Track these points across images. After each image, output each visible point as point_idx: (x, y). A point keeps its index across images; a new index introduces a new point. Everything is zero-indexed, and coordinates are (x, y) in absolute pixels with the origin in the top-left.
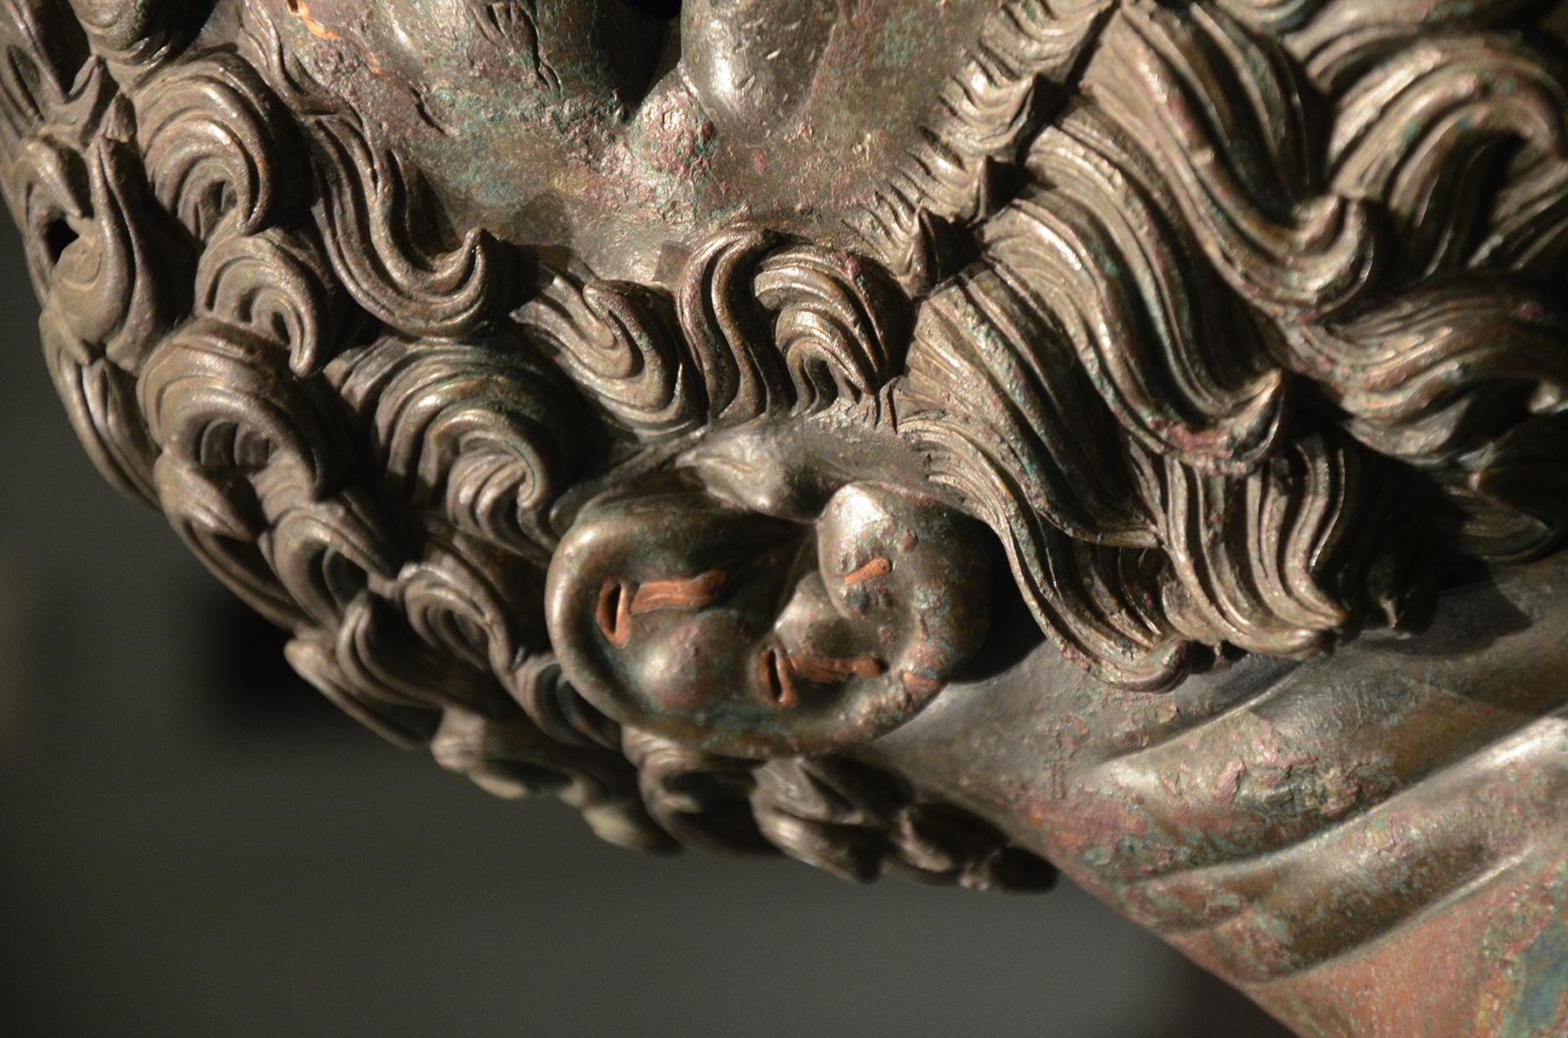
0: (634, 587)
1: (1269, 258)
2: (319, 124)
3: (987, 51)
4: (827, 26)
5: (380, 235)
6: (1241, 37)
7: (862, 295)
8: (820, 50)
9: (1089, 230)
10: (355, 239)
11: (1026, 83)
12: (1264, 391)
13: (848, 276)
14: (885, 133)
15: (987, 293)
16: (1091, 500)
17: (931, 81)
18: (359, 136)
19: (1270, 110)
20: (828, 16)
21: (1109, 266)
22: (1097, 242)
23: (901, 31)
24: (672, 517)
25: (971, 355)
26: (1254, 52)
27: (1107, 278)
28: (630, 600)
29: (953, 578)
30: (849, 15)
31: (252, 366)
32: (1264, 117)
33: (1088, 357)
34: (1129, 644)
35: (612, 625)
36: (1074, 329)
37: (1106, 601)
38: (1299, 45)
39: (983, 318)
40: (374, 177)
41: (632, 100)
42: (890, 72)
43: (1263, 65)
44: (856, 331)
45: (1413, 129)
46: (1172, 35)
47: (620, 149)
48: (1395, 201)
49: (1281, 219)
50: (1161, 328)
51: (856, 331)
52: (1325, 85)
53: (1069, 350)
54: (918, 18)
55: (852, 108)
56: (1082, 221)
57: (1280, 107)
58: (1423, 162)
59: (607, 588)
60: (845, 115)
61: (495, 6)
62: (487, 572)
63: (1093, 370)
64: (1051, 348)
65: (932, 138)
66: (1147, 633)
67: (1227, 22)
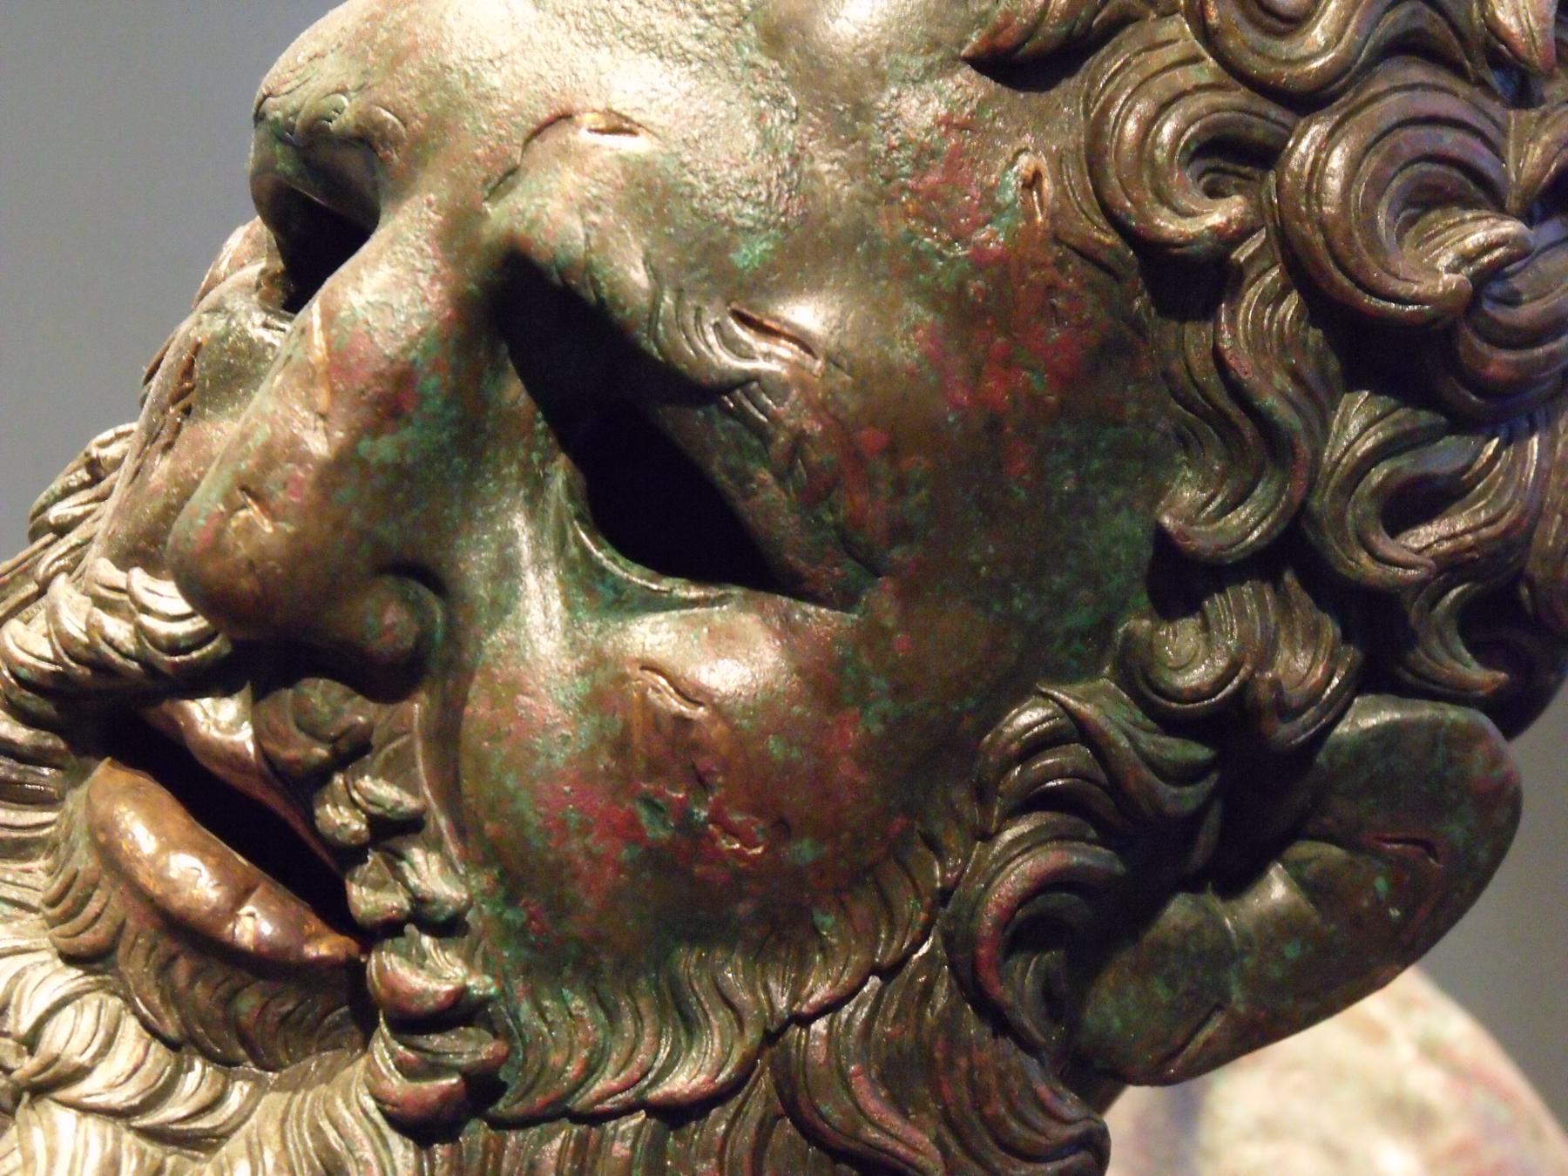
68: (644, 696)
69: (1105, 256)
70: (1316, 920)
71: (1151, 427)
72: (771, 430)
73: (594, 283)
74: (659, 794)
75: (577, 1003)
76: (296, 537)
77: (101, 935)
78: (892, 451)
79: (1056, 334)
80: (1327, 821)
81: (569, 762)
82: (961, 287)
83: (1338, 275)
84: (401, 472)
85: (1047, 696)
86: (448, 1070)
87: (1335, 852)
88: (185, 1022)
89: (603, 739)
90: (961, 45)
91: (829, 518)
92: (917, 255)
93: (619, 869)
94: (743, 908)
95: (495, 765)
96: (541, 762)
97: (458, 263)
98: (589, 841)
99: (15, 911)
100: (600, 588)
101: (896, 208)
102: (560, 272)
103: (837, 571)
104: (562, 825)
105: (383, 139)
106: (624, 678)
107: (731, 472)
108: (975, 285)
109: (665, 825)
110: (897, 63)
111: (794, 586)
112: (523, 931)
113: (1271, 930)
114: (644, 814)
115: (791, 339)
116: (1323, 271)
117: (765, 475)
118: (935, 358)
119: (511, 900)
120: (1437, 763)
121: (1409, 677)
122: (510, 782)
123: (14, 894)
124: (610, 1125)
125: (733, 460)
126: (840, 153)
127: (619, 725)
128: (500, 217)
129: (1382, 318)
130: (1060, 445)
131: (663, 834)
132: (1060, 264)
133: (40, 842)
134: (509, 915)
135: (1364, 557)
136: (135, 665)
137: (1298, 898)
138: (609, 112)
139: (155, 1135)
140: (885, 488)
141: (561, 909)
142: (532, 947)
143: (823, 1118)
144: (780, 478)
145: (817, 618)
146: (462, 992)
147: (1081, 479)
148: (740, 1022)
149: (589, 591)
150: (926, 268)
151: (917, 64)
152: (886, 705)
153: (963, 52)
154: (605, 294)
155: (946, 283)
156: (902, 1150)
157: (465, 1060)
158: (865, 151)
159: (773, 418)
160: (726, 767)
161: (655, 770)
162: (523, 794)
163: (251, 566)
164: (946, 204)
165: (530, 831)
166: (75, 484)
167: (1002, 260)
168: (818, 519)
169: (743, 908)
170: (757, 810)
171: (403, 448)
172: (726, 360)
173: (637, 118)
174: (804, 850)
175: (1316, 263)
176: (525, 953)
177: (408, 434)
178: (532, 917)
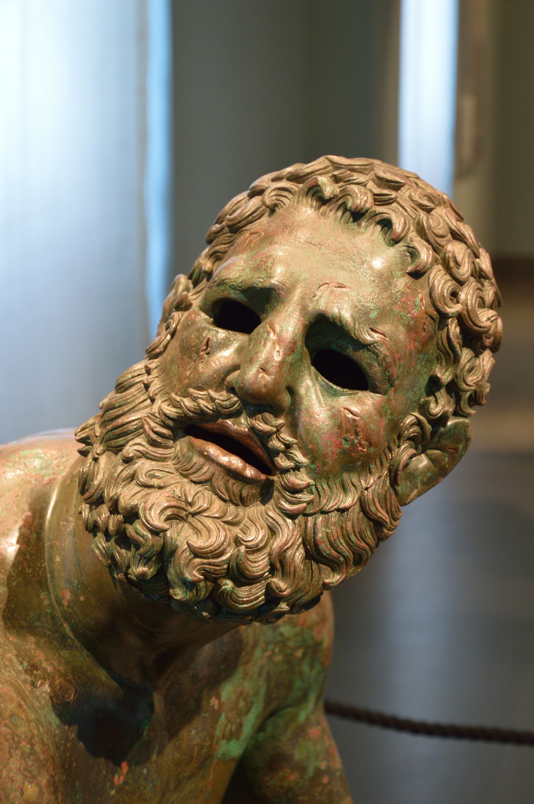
6: (128, 439)
9: (126, 402)
10: (220, 242)
13: (158, 350)
19: (116, 442)
21: (117, 405)
22: (122, 403)
26: (124, 441)
32: (114, 441)
39: (133, 377)
43: (121, 443)
44: (151, 349)
56: (129, 401)
65: (163, 372)
68: (345, 415)
69: (434, 317)
70: (433, 467)
71: (433, 355)
72: (380, 354)
73: (340, 321)
74: (348, 437)
75: (325, 487)
76: (275, 379)
77: (208, 476)
78: (400, 359)
79: (424, 334)
80: (439, 445)
81: (328, 430)
82: (409, 323)
83: (470, 322)
84: (292, 364)
85: (413, 415)
86: (303, 502)
87: (438, 452)
88: (229, 496)
89: (335, 425)
90: (406, 269)
91: (387, 374)
92: (401, 316)
93: (337, 455)
94: (359, 463)
95: (312, 432)
96: (322, 431)
97: (303, 317)
98: (332, 448)
99: (169, 474)
100: (331, 391)
101: (397, 305)
102: (333, 318)
103: (385, 386)
104: (327, 445)
105: (278, 289)
106: (340, 411)
107: (368, 364)
108: (412, 323)
109: (348, 444)
110: (395, 274)
111: (375, 390)
112: (315, 470)
113: (426, 470)
114: (344, 442)
115: (381, 334)
116: (467, 321)
117: (376, 364)
118: (405, 338)
119: (313, 463)
120: (462, 431)
121: (461, 412)
122: (316, 435)
124: (330, 514)
125: (369, 361)
126: (386, 293)
127: (340, 422)
129: (477, 332)
130: (419, 359)
131: (348, 446)
132: (426, 318)
133: (170, 458)
134: (312, 466)
135: (464, 385)
136: (211, 412)
137: (430, 462)
138: (338, 283)
139: (226, 522)
140: (397, 367)
141: (324, 464)
142: (317, 474)
143: (371, 511)
144: (379, 365)
145: (377, 397)
146: (309, 483)
147: (421, 366)
148: (356, 489)
149: (328, 392)
150: (403, 319)
151: (399, 273)
152: (389, 416)
153: (407, 271)
154: (344, 323)
155: (407, 323)
156: (384, 518)
157: (307, 500)
158: (391, 293)
159: (380, 352)
160: (363, 431)
161: (347, 431)
162: (319, 438)
163: (265, 386)
164: (407, 304)
165: (320, 446)
166: (136, 375)
167: (416, 317)
168: (386, 374)
169: (359, 463)
170: (367, 440)
171: (293, 359)
172: (368, 338)
173: (345, 284)
174: (372, 450)
175: (466, 319)
176: (314, 475)
177: (294, 356)
178: (318, 466)
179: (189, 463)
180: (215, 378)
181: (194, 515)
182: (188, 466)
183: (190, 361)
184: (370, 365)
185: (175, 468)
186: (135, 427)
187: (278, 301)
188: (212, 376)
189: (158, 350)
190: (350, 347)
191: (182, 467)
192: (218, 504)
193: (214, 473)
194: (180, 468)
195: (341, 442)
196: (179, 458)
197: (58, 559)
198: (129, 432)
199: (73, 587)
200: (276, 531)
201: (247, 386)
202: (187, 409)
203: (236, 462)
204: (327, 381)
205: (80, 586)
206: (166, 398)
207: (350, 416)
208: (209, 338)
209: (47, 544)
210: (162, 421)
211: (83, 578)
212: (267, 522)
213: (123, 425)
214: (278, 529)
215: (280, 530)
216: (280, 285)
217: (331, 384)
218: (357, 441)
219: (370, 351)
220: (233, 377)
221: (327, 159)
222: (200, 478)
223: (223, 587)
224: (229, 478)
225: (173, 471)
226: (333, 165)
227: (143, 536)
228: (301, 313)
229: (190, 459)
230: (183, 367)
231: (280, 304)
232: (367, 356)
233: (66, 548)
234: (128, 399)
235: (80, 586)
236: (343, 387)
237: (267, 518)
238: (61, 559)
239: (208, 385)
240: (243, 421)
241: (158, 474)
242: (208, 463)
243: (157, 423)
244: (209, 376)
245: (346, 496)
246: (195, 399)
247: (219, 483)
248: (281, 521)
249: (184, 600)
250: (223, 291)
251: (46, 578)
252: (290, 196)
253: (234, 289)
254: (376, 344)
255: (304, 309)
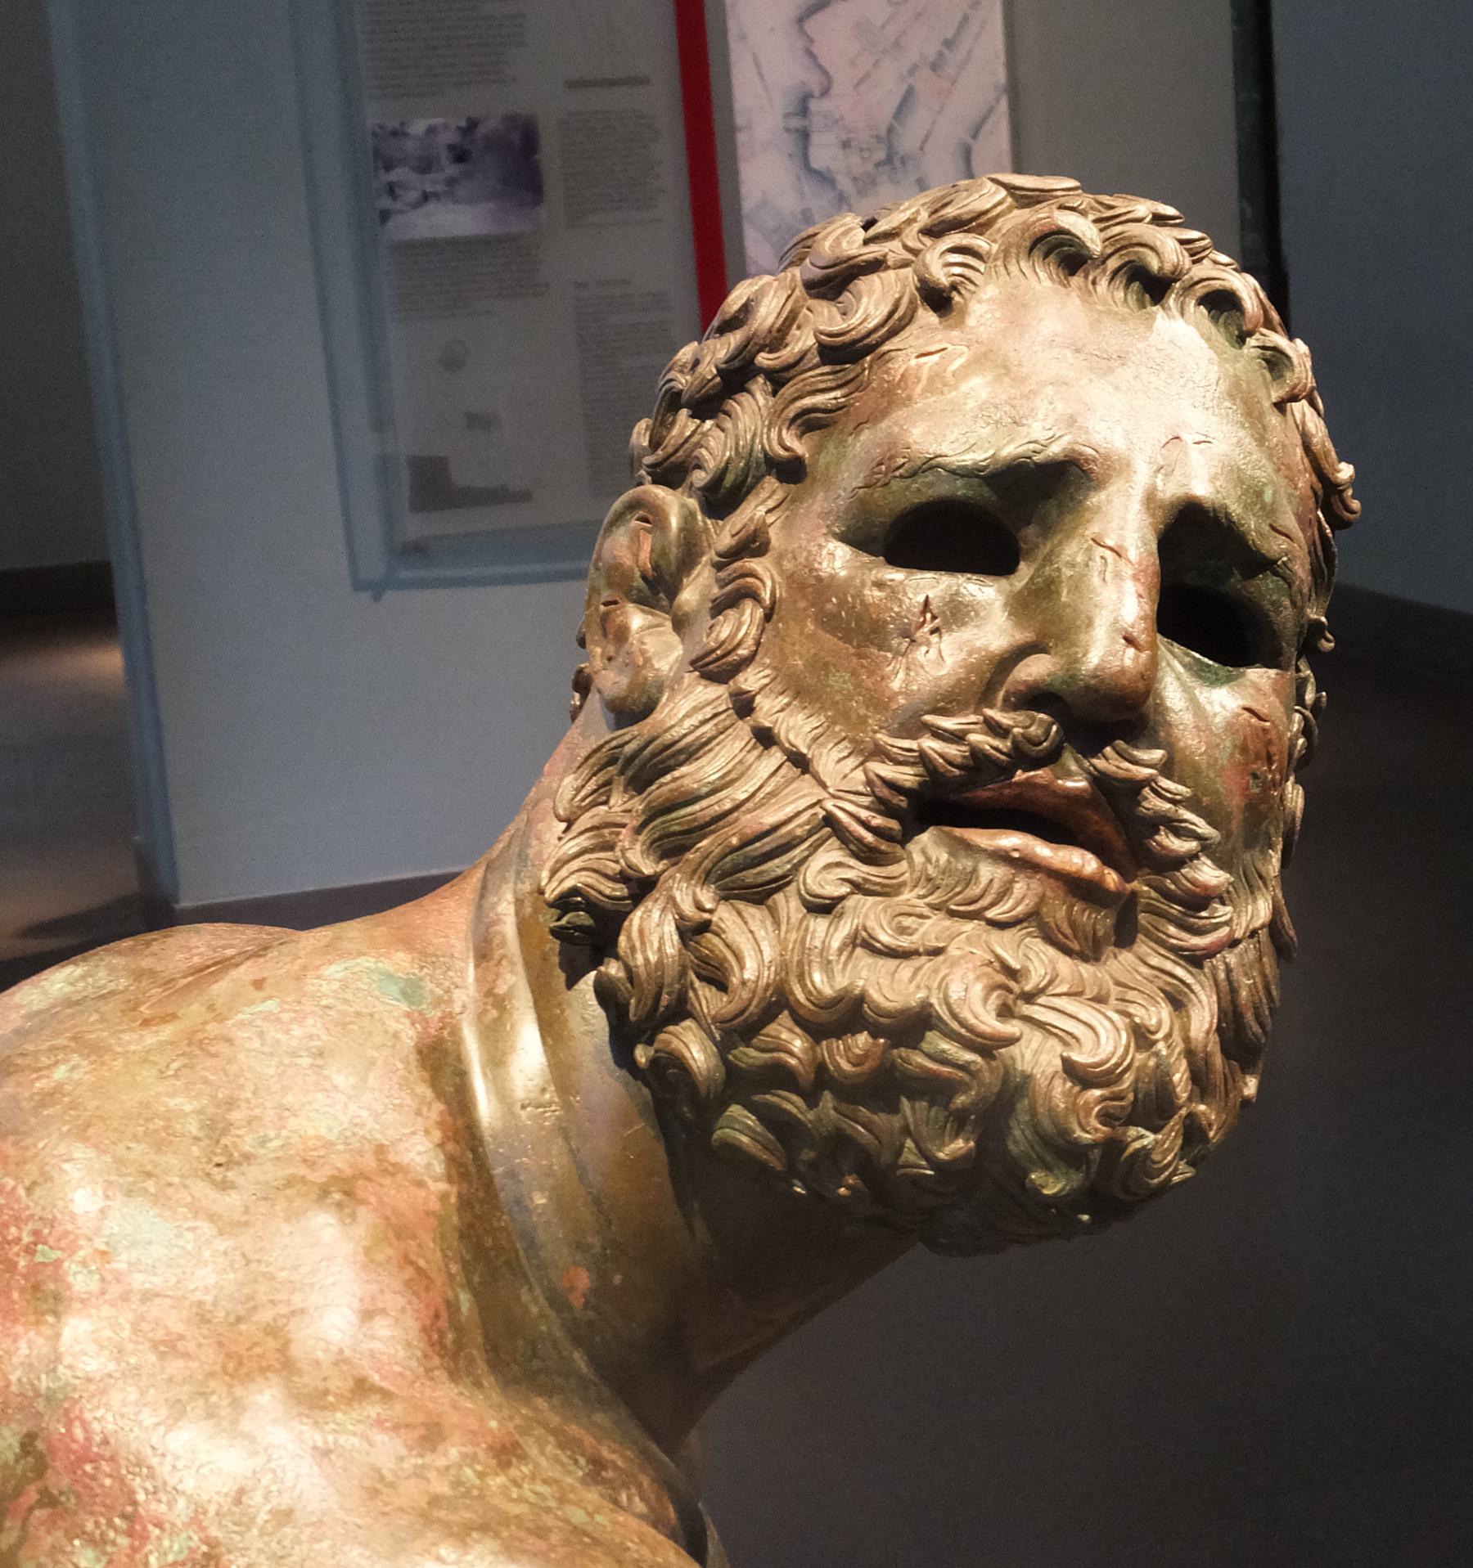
0: (649, 531)
1: (694, 872)
2: (864, 370)
3: (828, 727)
4: (850, 643)
5: (808, 402)
7: (730, 658)
8: (840, 639)
9: (728, 779)
10: (808, 388)
11: (804, 750)
12: (648, 868)
14: (802, 672)
15: (715, 725)
16: (630, 773)
17: (820, 697)
18: (856, 390)
20: (855, 643)
21: (705, 790)
23: (844, 682)
24: (674, 552)
25: (687, 716)
27: (699, 789)
28: (644, 529)
29: (630, 700)
30: (854, 655)
31: (770, 331)
33: (668, 777)
34: (578, 790)
35: (638, 519)
36: (684, 769)
37: (601, 777)
38: (791, 888)
39: (704, 722)
40: (835, 398)
41: (844, 538)
42: (827, 675)
43: (779, 872)
44: (714, 656)
45: (734, 947)
46: (800, 826)
47: (824, 531)
48: (709, 935)
49: (706, 879)
50: (674, 815)
51: (714, 656)
52: (770, 902)
53: (671, 769)
54: (849, 691)
55: (815, 654)
56: (733, 776)
57: (760, 880)
58: (721, 951)
59: (651, 517)
60: (813, 651)
61: (883, 467)
62: (681, 453)
63: (663, 780)
64: (682, 757)
66: (583, 799)
67: (806, 853)
73: (1227, 515)
97: (1153, 515)
100: (1209, 675)
102: (1214, 510)
105: (1087, 461)
107: (1273, 603)
117: (1287, 602)
122: (1212, 775)
123: (918, 910)
128: (1170, 490)
133: (902, 885)
149: (1201, 677)
161: (1258, 757)
179: (967, 885)
180: (973, 682)
181: (1029, 998)
182: (974, 890)
183: (889, 655)
184: (1277, 605)
185: (929, 905)
186: (807, 827)
187: (1089, 489)
188: (967, 679)
189: (743, 652)
190: (1236, 572)
191: (951, 898)
192: (1065, 964)
193: (1044, 895)
194: (947, 901)
195: (1248, 783)
196: (929, 880)
197: (540, 1199)
198: (794, 842)
199: (594, 1255)
200: (1185, 1000)
201: (1107, 681)
202: (945, 760)
203: (1081, 861)
204: (1197, 655)
205: (608, 1252)
206: (845, 754)
207: (1254, 720)
208: (927, 597)
209: (498, 1171)
210: (880, 800)
211: (614, 1228)
212: (1162, 984)
213: (775, 828)
214: (1186, 994)
215: (1192, 996)
216: (1089, 451)
217: (1206, 660)
218: (1270, 776)
219: (1276, 574)
220: (1035, 669)
221: (993, 180)
222: (1013, 913)
223: (1137, 1145)
224: (1074, 900)
225: (926, 911)
226: (1012, 195)
227: (964, 1067)
228: (1148, 508)
229: (971, 877)
230: (871, 673)
231: (1092, 494)
232: (1271, 586)
233: (555, 1168)
234: (730, 772)
235: (608, 1252)
236: (1225, 664)
237: (1157, 977)
238: (550, 1198)
239: (958, 702)
240: (1074, 767)
241: (908, 922)
242: (1022, 876)
243: (867, 808)
244: (959, 680)
245: (1255, 900)
246: (957, 737)
247: (1059, 912)
248: (1189, 979)
249: (1063, 1193)
250: (931, 485)
251: (516, 1252)
252: (981, 266)
253: (962, 476)
254: (1285, 559)
255: (1150, 498)
